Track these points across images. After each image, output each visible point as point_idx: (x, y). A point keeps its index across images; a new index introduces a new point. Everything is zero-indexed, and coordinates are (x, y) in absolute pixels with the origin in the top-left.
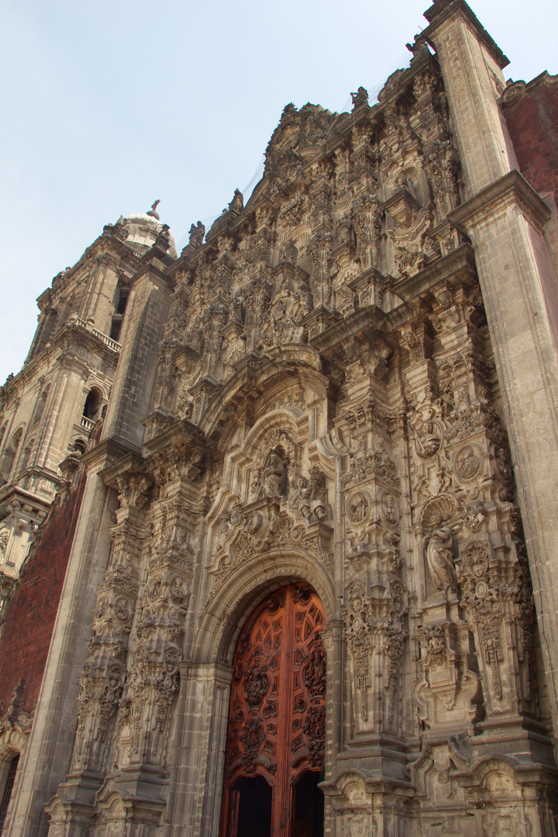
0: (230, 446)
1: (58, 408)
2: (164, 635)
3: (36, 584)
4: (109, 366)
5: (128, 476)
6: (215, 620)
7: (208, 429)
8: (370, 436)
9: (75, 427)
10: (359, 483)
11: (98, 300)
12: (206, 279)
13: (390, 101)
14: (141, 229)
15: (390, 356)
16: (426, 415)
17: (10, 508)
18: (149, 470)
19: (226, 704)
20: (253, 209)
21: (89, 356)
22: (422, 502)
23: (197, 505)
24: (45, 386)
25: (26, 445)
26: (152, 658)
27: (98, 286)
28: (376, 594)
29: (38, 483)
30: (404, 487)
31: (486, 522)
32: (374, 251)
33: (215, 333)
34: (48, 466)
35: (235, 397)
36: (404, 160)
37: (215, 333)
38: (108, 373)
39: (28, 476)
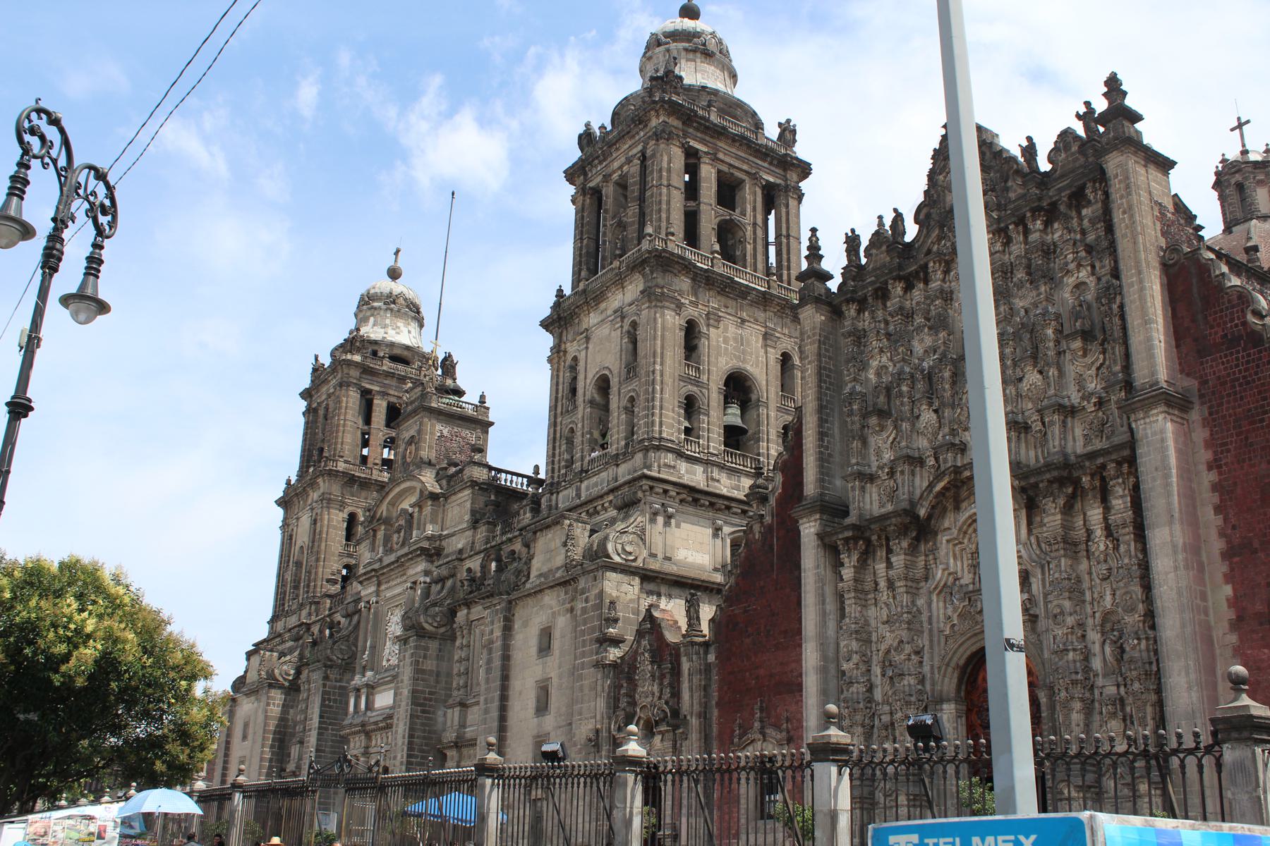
0: (942, 528)
2: (912, 681)
3: (746, 611)
4: (700, 286)
5: (847, 540)
6: (950, 669)
7: (922, 512)
8: (1063, 560)
9: (682, 379)
10: (1057, 597)
11: (669, 195)
12: (879, 322)
13: (1063, 194)
14: (686, 50)
16: (1102, 547)
17: (640, 494)
18: (867, 534)
19: (965, 728)
20: (925, 260)
21: (676, 280)
22: (1101, 609)
23: (919, 572)
24: (627, 322)
25: (624, 402)
26: (907, 698)
27: (665, 174)
28: (1074, 677)
29: (660, 458)
30: (1088, 597)
31: (1139, 644)
32: (1056, 373)
33: (906, 400)
34: (664, 435)
35: (944, 488)
36: (1078, 272)
37: (906, 400)
38: (700, 295)
39: (647, 450)
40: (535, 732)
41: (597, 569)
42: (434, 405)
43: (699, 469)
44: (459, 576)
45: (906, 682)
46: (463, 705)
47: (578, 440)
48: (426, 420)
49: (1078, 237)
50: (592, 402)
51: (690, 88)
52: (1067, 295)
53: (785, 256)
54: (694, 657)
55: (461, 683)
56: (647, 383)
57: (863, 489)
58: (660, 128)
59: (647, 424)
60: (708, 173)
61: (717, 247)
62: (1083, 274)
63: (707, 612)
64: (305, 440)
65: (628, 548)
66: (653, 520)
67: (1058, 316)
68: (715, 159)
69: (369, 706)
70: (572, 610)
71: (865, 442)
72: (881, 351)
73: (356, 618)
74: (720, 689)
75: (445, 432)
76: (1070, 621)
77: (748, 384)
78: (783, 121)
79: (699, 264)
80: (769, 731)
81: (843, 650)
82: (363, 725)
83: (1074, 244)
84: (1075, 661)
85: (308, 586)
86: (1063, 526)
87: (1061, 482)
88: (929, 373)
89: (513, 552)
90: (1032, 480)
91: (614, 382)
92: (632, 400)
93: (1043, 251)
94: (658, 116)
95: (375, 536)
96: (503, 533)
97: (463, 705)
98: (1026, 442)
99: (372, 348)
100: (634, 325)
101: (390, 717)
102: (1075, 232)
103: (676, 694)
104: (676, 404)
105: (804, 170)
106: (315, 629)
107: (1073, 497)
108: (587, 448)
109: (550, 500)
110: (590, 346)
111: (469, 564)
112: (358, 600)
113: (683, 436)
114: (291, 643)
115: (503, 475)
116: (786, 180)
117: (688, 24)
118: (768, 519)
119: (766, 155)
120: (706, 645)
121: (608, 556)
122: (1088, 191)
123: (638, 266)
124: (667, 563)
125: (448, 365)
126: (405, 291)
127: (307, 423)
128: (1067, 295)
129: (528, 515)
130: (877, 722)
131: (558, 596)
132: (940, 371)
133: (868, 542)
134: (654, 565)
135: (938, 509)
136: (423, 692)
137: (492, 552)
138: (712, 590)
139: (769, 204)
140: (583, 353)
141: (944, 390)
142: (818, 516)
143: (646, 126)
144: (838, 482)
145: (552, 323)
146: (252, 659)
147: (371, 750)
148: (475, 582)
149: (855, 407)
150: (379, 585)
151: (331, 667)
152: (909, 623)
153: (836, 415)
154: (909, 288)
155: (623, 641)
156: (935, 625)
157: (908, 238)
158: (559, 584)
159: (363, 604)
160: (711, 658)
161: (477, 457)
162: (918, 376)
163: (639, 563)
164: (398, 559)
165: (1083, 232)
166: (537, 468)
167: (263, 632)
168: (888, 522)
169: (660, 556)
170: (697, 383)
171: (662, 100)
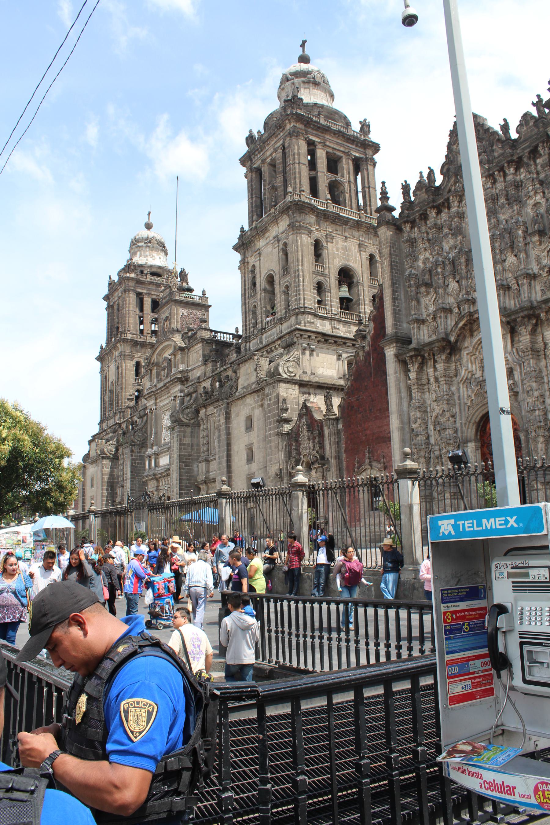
1: (300, 263)
2: (451, 432)
3: (358, 400)
5: (411, 357)
6: (471, 424)
7: (452, 339)
8: (531, 361)
9: (314, 273)
10: (529, 381)
11: (300, 168)
14: (304, 82)
15: (537, 321)
17: (295, 339)
18: (422, 353)
21: (307, 217)
23: (452, 372)
24: (281, 243)
25: (283, 288)
27: (296, 156)
28: (539, 424)
32: (524, 256)
33: (440, 276)
34: (306, 305)
35: (465, 325)
38: (321, 225)
39: (297, 314)
40: (247, 472)
41: (274, 382)
42: (177, 298)
43: (327, 323)
44: (199, 392)
45: (447, 433)
46: (207, 461)
47: (258, 312)
48: (174, 307)
49: (535, 176)
50: (265, 290)
51: (307, 105)
52: (529, 211)
53: (368, 199)
54: (331, 427)
55: (205, 449)
56: (295, 277)
57: (419, 328)
58: (292, 130)
59: (296, 300)
60: (321, 154)
61: (329, 197)
62: (538, 198)
63: (336, 401)
64: (108, 323)
65: (291, 370)
66: (303, 353)
67: (524, 223)
68: (325, 145)
69: (157, 465)
70: (262, 405)
71: (418, 302)
72: (425, 249)
73: (145, 418)
74: (346, 443)
75: (185, 313)
76: (536, 394)
77: (351, 273)
78: (362, 120)
79: (319, 207)
80: (374, 464)
81: (412, 418)
82: (154, 475)
83: (533, 180)
84: (539, 416)
85: (118, 403)
86: (531, 342)
87: (529, 317)
88: (453, 260)
89: (228, 376)
90: (513, 317)
91: (276, 278)
92: (287, 287)
93: (515, 186)
94: (290, 123)
95: (151, 373)
96: (221, 366)
97: (207, 461)
98: (509, 296)
99: (140, 269)
100: (285, 244)
101: (169, 470)
102: (533, 173)
103: (322, 447)
104: (312, 287)
105: (376, 148)
106: (124, 426)
107: (536, 325)
108: (264, 316)
109: (246, 346)
110: (262, 258)
111: (204, 384)
112: (145, 409)
113: (317, 305)
114: (112, 434)
115: (219, 334)
116: (366, 155)
117: (304, 67)
118: (367, 348)
119: (354, 141)
120: (337, 419)
121: (280, 375)
122: (540, 149)
123: (285, 210)
124: (313, 376)
125: (183, 276)
126: (156, 236)
127: (108, 314)
128: (529, 211)
129: (234, 355)
130: (432, 455)
131: (254, 398)
132: (459, 259)
133: (423, 357)
134: (306, 378)
135: (461, 337)
136: (185, 455)
137: (216, 377)
138: (338, 389)
139: (357, 169)
140: (258, 262)
141: (462, 269)
142: (394, 345)
143: (284, 129)
144: (405, 325)
145: (239, 247)
146: (92, 444)
147: (160, 488)
148: (208, 394)
149: (412, 282)
150: (156, 399)
151: (134, 445)
152: (447, 400)
153: (402, 287)
154: (439, 212)
155: (291, 421)
156: (462, 401)
157: (437, 184)
158: (254, 392)
159: (148, 411)
160: (340, 426)
161: (204, 325)
162: (447, 262)
163: (297, 377)
164: (165, 384)
165: (538, 173)
166: (237, 329)
167: (96, 430)
168: (434, 346)
169: (309, 372)
170: (323, 275)
171: (292, 113)
